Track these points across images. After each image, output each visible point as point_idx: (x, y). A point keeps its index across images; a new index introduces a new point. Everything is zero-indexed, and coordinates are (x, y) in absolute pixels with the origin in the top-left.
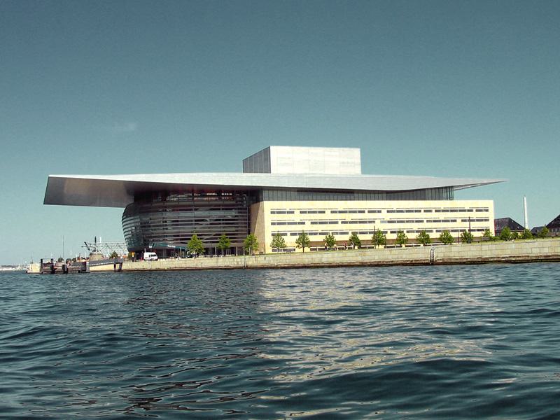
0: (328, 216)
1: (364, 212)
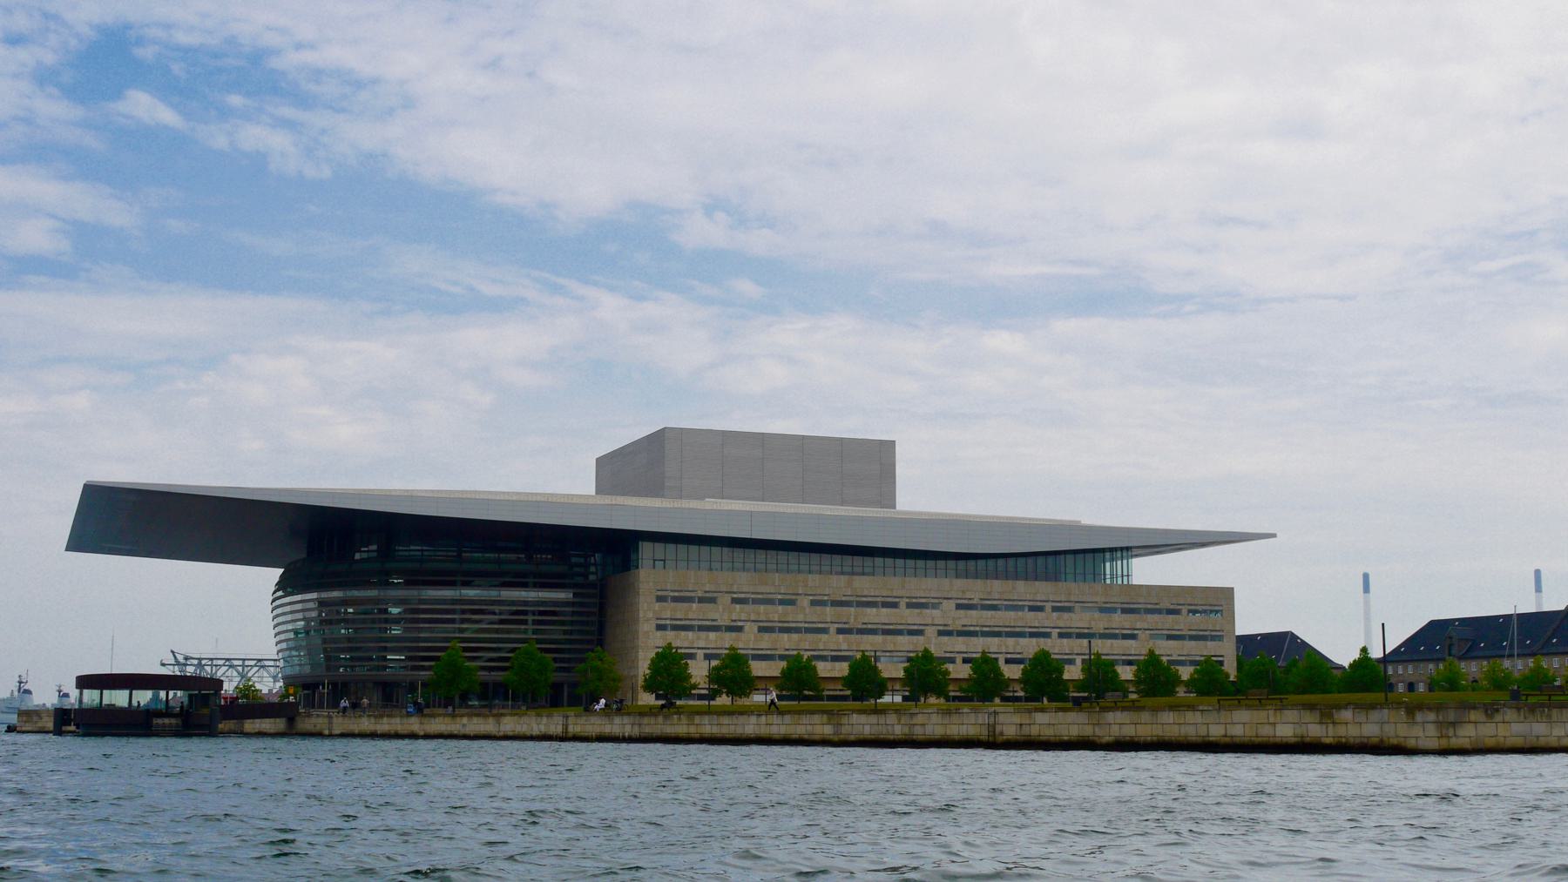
0: (804, 613)
1: (895, 605)
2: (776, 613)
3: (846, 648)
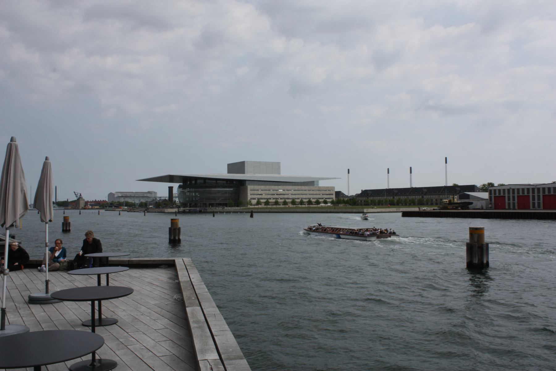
0: (272, 192)
2: (267, 192)
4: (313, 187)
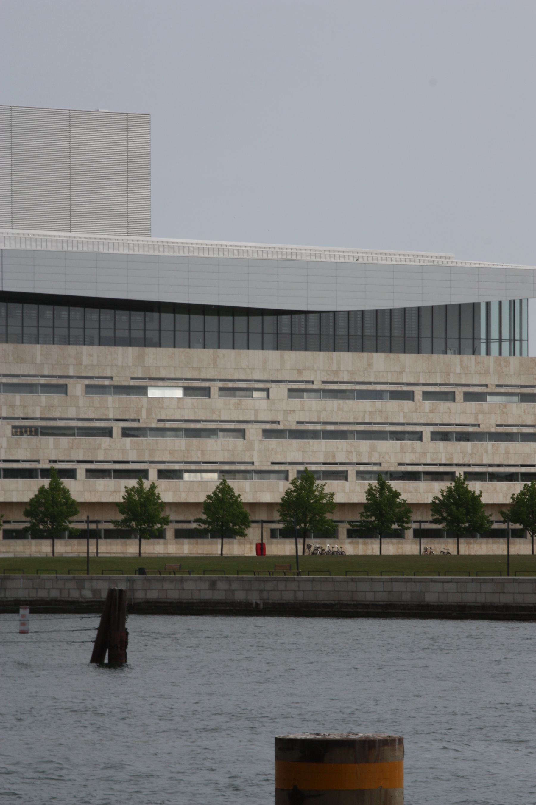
3: (135, 459)
4: (469, 360)
